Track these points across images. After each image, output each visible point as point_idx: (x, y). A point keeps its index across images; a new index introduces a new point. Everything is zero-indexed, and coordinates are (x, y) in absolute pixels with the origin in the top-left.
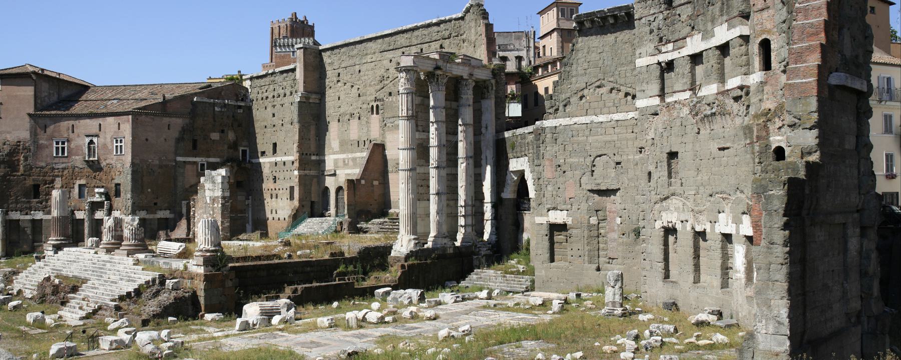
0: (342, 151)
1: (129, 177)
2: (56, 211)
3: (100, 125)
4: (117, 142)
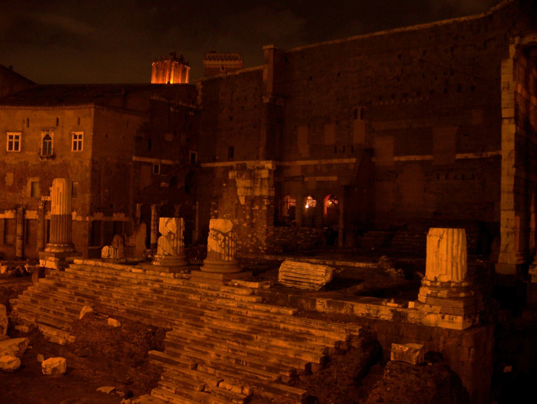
0: (311, 158)
1: (88, 175)
2: (58, 207)
3: (58, 120)
4: (75, 137)
